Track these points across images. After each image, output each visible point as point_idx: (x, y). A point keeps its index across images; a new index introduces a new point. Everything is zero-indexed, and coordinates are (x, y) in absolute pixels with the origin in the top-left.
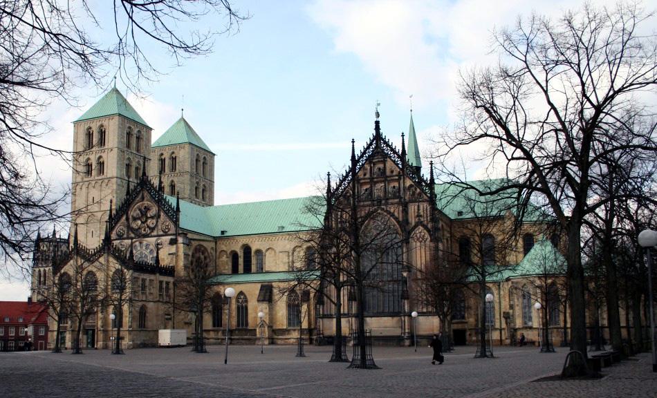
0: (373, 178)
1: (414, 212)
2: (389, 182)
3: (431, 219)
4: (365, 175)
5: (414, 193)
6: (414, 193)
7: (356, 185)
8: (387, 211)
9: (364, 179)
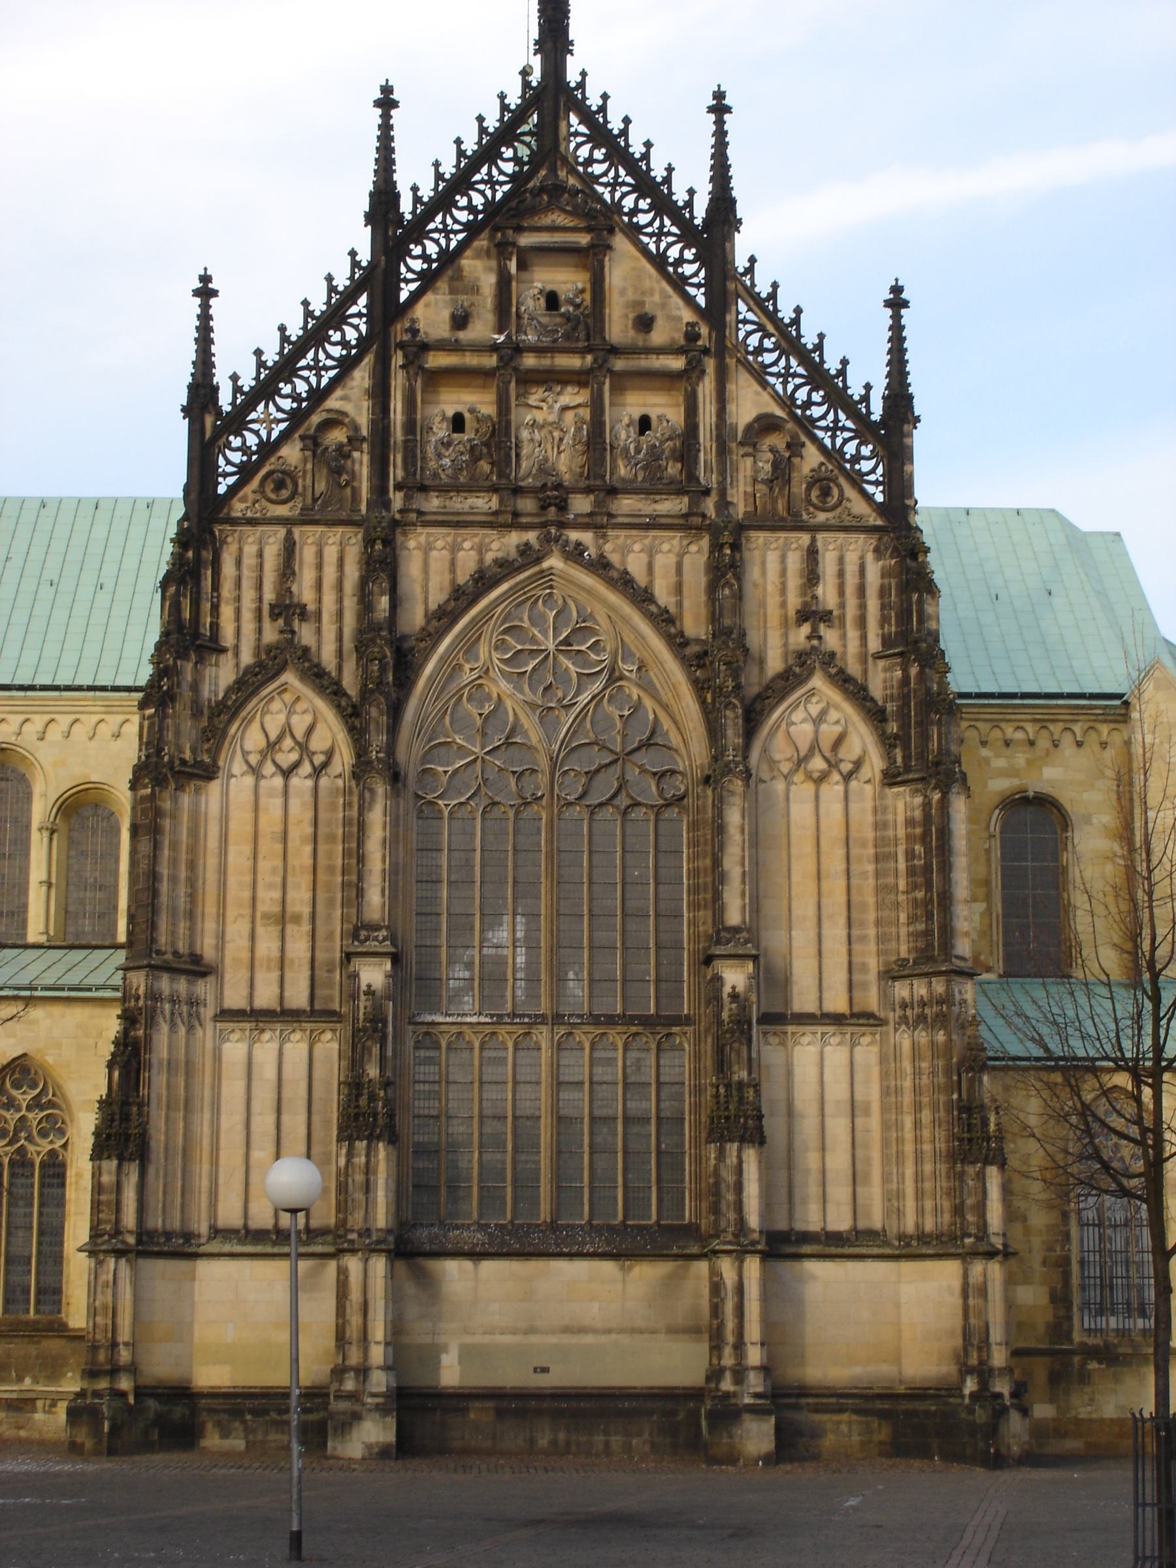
0: (519, 349)
1: (783, 590)
2: (623, 382)
3: (886, 641)
4: (460, 321)
5: (782, 471)
6: (782, 471)
7: (398, 381)
8: (600, 566)
9: (455, 347)
